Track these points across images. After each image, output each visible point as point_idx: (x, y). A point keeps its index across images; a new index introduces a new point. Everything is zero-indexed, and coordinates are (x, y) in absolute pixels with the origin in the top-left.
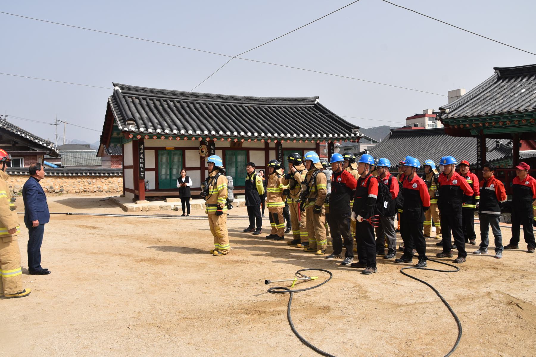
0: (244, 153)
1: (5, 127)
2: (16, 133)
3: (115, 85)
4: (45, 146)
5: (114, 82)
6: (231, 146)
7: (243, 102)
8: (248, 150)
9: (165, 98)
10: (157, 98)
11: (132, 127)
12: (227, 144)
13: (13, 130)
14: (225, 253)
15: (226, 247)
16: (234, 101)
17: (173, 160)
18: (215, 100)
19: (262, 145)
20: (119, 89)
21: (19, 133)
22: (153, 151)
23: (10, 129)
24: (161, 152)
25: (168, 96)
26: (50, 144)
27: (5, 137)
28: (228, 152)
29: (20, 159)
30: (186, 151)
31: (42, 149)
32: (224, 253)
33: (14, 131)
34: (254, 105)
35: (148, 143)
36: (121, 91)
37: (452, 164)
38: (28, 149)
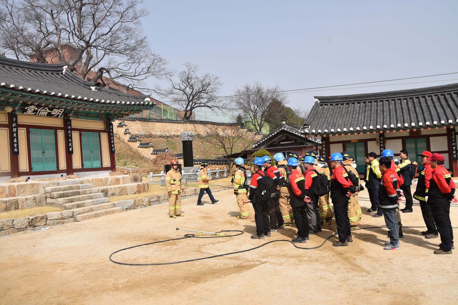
0: (424, 139)
1: (288, 130)
3: (316, 97)
5: (315, 96)
6: (410, 135)
7: (426, 93)
8: (427, 138)
9: (353, 101)
10: (347, 102)
11: (307, 130)
12: (406, 133)
16: (417, 93)
18: (397, 96)
19: (444, 130)
20: (318, 100)
21: (296, 134)
22: (342, 144)
23: (291, 131)
24: (347, 145)
25: (355, 100)
27: (291, 137)
28: (407, 141)
29: (285, 153)
30: (368, 142)
32: (243, 218)
33: (294, 133)
34: (438, 94)
35: (332, 139)
36: (319, 102)
37: (334, 161)
38: (303, 144)
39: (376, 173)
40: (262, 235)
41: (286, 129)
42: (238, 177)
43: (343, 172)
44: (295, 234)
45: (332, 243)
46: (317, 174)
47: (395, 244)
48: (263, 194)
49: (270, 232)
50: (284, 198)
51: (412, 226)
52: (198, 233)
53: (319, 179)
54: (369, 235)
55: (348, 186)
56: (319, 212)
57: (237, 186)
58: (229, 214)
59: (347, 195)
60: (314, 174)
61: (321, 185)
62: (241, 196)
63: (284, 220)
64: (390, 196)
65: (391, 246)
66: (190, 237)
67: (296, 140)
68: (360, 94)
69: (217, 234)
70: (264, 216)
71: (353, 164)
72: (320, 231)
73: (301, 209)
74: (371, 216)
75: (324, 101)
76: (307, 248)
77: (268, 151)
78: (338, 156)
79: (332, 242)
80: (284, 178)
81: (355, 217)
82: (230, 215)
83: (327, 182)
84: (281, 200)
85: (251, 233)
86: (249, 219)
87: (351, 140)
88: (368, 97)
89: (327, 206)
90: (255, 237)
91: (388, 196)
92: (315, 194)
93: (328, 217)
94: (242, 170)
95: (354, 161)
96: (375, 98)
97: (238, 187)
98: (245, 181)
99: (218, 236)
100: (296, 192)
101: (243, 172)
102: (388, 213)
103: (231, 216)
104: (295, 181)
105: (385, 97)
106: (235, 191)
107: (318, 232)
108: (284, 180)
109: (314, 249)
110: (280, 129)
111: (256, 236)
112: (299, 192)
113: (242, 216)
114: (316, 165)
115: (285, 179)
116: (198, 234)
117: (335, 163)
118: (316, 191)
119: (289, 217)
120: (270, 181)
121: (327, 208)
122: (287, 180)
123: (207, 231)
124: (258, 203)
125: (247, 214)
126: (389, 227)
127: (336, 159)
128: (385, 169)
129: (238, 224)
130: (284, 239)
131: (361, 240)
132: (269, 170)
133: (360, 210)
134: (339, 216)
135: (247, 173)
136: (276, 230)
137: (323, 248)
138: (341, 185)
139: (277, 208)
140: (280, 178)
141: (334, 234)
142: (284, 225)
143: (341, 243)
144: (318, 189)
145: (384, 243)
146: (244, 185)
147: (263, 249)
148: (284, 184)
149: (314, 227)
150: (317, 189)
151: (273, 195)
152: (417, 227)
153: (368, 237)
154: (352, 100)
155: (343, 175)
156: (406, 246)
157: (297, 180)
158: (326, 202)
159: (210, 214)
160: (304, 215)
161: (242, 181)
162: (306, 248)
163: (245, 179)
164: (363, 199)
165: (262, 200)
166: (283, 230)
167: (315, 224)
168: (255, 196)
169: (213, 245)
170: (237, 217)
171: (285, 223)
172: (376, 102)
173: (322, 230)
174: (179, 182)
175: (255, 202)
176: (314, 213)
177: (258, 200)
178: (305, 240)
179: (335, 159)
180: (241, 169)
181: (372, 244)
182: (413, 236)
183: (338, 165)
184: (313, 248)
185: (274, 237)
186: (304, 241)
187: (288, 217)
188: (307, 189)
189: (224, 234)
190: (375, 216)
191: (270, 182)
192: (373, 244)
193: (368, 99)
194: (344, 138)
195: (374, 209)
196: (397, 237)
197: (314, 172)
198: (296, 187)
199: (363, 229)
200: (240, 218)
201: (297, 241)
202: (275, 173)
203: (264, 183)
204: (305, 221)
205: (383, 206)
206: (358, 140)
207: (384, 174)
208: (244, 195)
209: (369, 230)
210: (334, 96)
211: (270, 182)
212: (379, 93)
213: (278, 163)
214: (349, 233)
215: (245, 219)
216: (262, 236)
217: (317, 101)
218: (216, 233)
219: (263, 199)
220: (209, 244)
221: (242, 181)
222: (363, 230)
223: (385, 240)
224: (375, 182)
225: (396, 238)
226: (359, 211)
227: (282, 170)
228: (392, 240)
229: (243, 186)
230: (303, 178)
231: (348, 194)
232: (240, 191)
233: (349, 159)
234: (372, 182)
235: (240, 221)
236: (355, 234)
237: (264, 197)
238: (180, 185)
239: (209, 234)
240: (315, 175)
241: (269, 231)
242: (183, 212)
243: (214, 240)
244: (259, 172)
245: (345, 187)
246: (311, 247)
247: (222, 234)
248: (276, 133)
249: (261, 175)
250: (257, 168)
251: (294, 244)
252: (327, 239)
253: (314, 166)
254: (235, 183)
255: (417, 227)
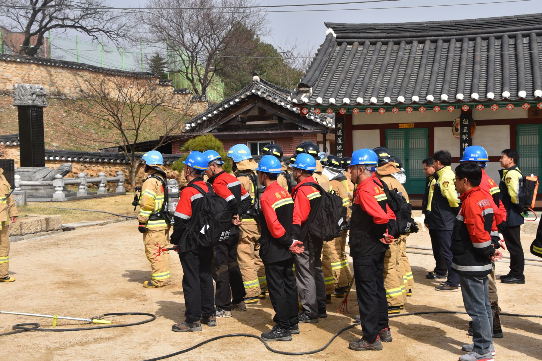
1: (265, 96)
2: (279, 104)
3: (328, 25)
4: (318, 122)
6: (529, 115)
9: (410, 37)
10: (395, 40)
11: (305, 97)
13: (276, 99)
14: (157, 285)
15: (158, 276)
17: (411, 146)
18: (508, 29)
20: (333, 32)
21: (283, 104)
22: (378, 132)
23: (270, 99)
24: (390, 133)
25: (415, 34)
26: (326, 118)
27: (270, 111)
28: (521, 128)
29: (257, 144)
30: (436, 129)
31: (315, 126)
33: (277, 101)
36: (335, 35)
37: (357, 165)
39: (448, 197)
40: (197, 323)
41: (259, 93)
42: (149, 193)
43: (377, 191)
44: (270, 323)
45: (348, 344)
46: (321, 193)
47: (484, 351)
48: (203, 231)
49: (215, 315)
50: (249, 244)
51: (522, 313)
52: (49, 320)
53: (323, 203)
54: (428, 328)
55: (385, 220)
56: (322, 274)
57: (146, 214)
58: (124, 276)
59: (383, 241)
60: (314, 192)
61: (327, 216)
62: (154, 235)
63: (247, 290)
64: (476, 245)
65: (475, 354)
66: (26, 330)
67: (280, 119)
68: (427, 23)
69: (95, 321)
70: (203, 281)
71: (400, 175)
72: (324, 315)
73: (282, 268)
74: (434, 288)
75: (346, 35)
76: (295, 352)
77: (219, 140)
78: (366, 157)
79: (349, 341)
80: (249, 198)
81: (399, 289)
82: (128, 278)
83: (340, 210)
84: (242, 247)
85: (173, 319)
86: (170, 288)
87: (398, 124)
88: (443, 29)
89: (340, 263)
90: (180, 327)
91: (472, 246)
92: (314, 236)
93: (341, 286)
94: (159, 179)
95: (402, 168)
96: (458, 32)
97: (148, 215)
98: (165, 202)
99: (96, 326)
100: (275, 230)
101: (160, 183)
102: (470, 283)
103: (130, 281)
104: (273, 206)
105: (480, 31)
106: (140, 223)
107: (319, 319)
108: (251, 203)
109: (308, 356)
110: (247, 91)
111: (184, 326)
112: (279, 231)
113: (153, 280)
114: (319, 173)
115: (253, 202)
116: (48, 323)
117: (359, 171)
118: (316, 228)
119: (258, 285)
120: (221, 205)
121: (340, 267)
122: (255, 204)
123: (72, 315)
124: (191, 251)
125: (166, 277)
126: (471, 312)
127: (363, 163)
128: (469, 188)
129: (144, 299)
130: (244, 333)
131: (410, 337)
132: (218, 180)
133: (411, 273)
134: (363, 285)
135: (169, 186)
136: (229, 312)
137: (327, 354)
138: (370, 218)
139: (233, 264)
140: (243, 198)
141: (352, 324)
142: (246, 302)
143: (366, 344)
144: (321, 226)
145: (460, 348)
146: (162, 210)
147: (197, 355)
148: (248, 212)
149: (310, 308)
150: (319, 225)
151: (224, 235)
152: (535, 316)
153: (426, 332)
154: (408, 34)
155: (376, 197)
156: (509, 356)
157: (277, 204)
158: (338, 254)
159: (81, 275)
160: (290, 281)
161: (159, 203)
162: (292, 352)
163: (165, 198)
164: (417, 250)
165: (200, 245)
166: (243, 313)
167: (312, 301)
168: (186, 236)
169: (84, 348)
170: (142, 282)
171: (248, 298)
172: (461, 40)
173: (328, 313)
174: (5, 202)
175: (184, 250)
176: (310, 276)
177: (190, 246)
178: (290, 335)
179: (360, 163)
180: (156, 175)
181: (433, 347)
182: (524, 336)
183: (366, 176)
184: (306, 353)
185: (223, 327)
186: (288, 338)
187: (255, 284)
188: (297, 225)
189: (110, 322)
190: (441, 288)
191: (220, 207)
192: (436, 348)
193: (443, 33)
194: (383, 118)
195: (440, 272)
196: (488, 336)
197: (314, 189)
198: (273, 218)
199: (416, 314)
200: (150, 284)
201: (273, 338)
202: (230, 189)
203: (207, 208)
204: (290, 292)
205: (460, 266)
206: (415, 123)
207: (466, 198)
208: (160, 234)
209: (427, 318)
210: (369, 25)
211: (220, 207)
212: (469, 21)
213: (237, 165)
214: (384, 322)
215: (162, 287)
216: (197, 326)
217: (330, 34)
218: (92, 319)
219: (202, 243)
220: (72, 346)
221: (159, 203)
222: (416, 317)
223: (461, 341)
224: (445, 214)
225: (486, 339)
226: (408, 276)
227: (245, 181)
228: (478, 342)
229: (159, 215)
230: (289, 201)
231: (384, 237)
232: (152, 225)
233: (391, 163)
234: (439, 215)
235: (150, 292)
236: (400, 325)
237: (205, 239)
238: (5, 209)
239: (74, 322)
240: (315, 194)
241: (213, 313)
242: (13, 273)
243: (86, 336)
244: (196, 183)
245: (378, 222)
246: (303, 351)
247: (107, 321)
248: (237, 100)
249: (200, 191)
250: (192, 174)
251: (265, 344)
252: (338, 335)
253: (315, 175)
254: (141, 206)
255: (535, 316)
